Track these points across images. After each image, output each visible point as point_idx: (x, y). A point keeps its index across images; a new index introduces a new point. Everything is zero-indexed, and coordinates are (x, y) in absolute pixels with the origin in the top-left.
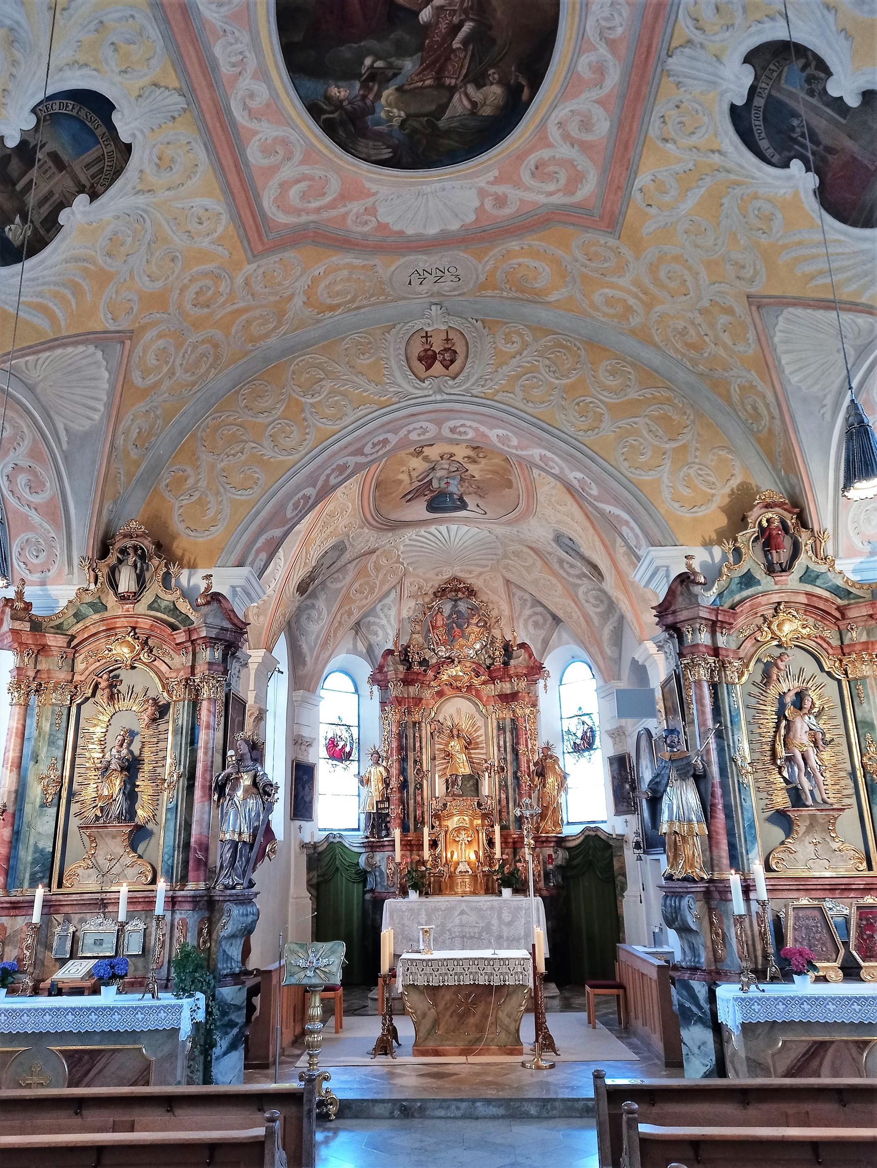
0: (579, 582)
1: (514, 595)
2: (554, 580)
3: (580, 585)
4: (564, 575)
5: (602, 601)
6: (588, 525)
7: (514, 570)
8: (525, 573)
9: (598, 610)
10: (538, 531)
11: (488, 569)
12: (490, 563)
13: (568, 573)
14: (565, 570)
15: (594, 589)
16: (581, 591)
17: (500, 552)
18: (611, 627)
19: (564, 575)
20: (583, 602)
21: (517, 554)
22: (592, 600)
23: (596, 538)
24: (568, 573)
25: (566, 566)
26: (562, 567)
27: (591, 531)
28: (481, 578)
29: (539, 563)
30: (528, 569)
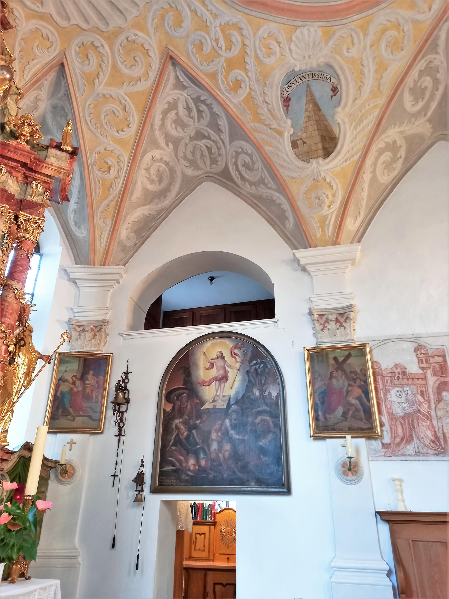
0: (163, 144)
1: (40, 88)
2: (135, 118)
3: (158, 147)
4: (157, 122)
5: (160, 181)
6: (387, 91)
7: (94, 59)
8: (105, 77)
9: (150, 187)
10: (301, 47)
11: (63, 23)
12: (77, 20)
13: (163, 124)
14: (163, 120)
15: (167, 164)
16: (157, 153)
17: (116, 21)
18: (146, 213)
19: (157, 122)
20: (144, 166)
21: (134, 49)
22: (153, 172)
23: (376, 113)
24: (163, 124)
25: (172, 115)
26: (165, 113)
27: (382, 101)
28: (33, 24)
29: (145, 86)
30: (117, 78)
